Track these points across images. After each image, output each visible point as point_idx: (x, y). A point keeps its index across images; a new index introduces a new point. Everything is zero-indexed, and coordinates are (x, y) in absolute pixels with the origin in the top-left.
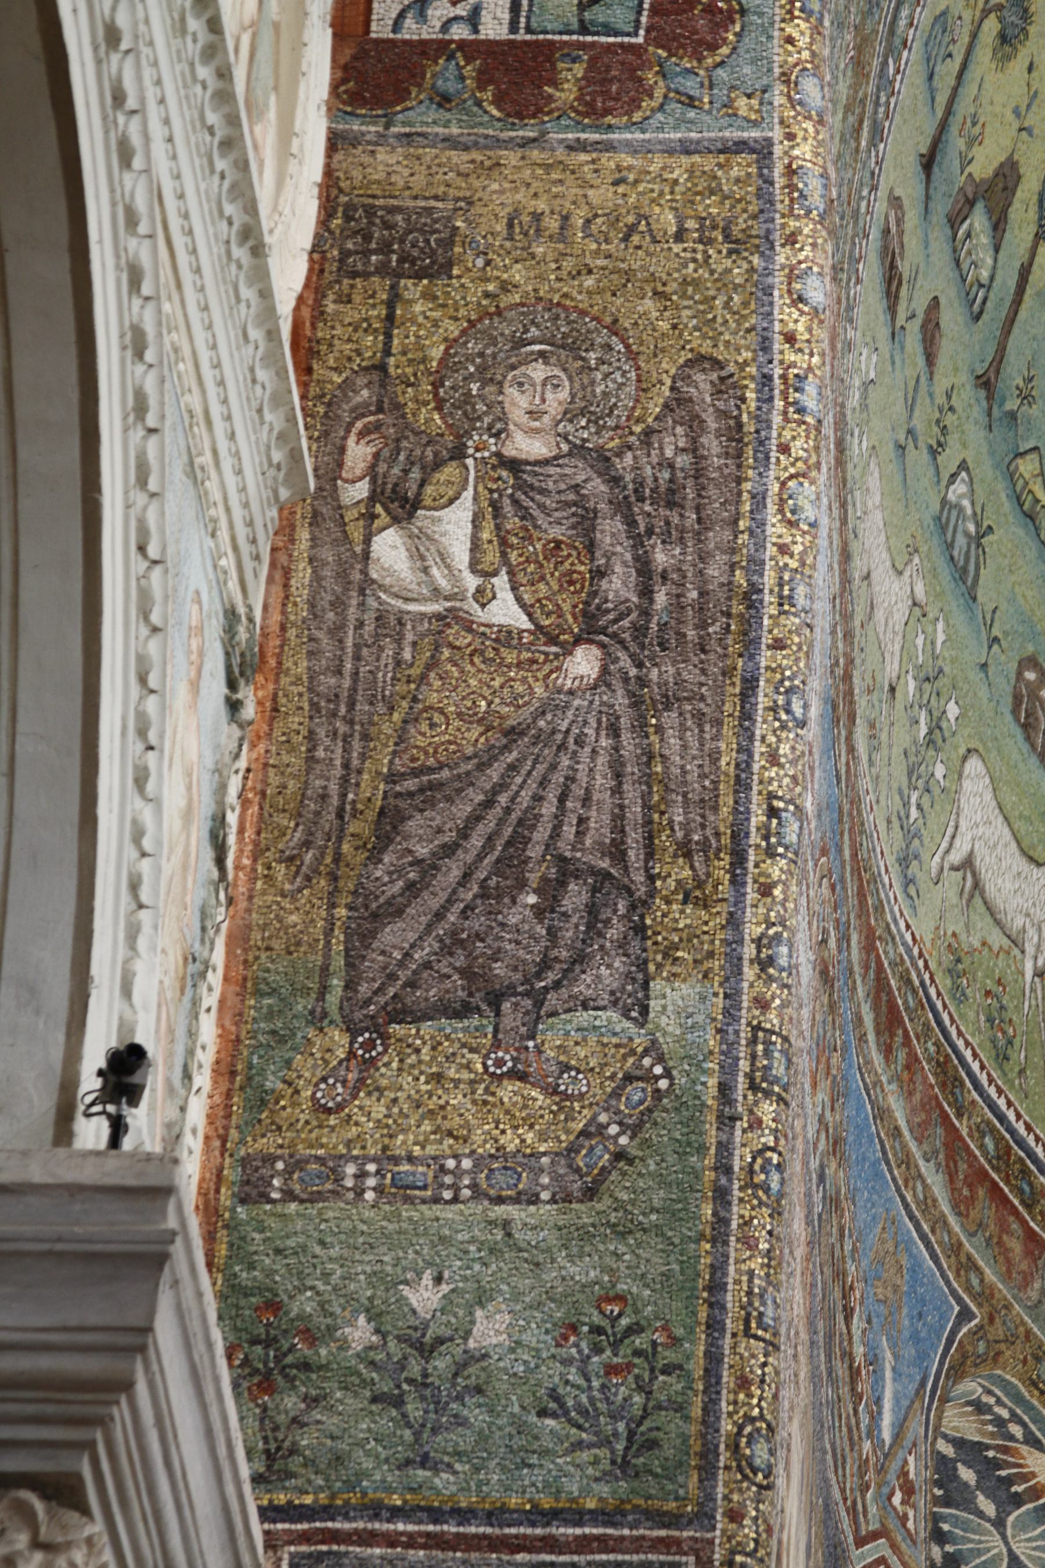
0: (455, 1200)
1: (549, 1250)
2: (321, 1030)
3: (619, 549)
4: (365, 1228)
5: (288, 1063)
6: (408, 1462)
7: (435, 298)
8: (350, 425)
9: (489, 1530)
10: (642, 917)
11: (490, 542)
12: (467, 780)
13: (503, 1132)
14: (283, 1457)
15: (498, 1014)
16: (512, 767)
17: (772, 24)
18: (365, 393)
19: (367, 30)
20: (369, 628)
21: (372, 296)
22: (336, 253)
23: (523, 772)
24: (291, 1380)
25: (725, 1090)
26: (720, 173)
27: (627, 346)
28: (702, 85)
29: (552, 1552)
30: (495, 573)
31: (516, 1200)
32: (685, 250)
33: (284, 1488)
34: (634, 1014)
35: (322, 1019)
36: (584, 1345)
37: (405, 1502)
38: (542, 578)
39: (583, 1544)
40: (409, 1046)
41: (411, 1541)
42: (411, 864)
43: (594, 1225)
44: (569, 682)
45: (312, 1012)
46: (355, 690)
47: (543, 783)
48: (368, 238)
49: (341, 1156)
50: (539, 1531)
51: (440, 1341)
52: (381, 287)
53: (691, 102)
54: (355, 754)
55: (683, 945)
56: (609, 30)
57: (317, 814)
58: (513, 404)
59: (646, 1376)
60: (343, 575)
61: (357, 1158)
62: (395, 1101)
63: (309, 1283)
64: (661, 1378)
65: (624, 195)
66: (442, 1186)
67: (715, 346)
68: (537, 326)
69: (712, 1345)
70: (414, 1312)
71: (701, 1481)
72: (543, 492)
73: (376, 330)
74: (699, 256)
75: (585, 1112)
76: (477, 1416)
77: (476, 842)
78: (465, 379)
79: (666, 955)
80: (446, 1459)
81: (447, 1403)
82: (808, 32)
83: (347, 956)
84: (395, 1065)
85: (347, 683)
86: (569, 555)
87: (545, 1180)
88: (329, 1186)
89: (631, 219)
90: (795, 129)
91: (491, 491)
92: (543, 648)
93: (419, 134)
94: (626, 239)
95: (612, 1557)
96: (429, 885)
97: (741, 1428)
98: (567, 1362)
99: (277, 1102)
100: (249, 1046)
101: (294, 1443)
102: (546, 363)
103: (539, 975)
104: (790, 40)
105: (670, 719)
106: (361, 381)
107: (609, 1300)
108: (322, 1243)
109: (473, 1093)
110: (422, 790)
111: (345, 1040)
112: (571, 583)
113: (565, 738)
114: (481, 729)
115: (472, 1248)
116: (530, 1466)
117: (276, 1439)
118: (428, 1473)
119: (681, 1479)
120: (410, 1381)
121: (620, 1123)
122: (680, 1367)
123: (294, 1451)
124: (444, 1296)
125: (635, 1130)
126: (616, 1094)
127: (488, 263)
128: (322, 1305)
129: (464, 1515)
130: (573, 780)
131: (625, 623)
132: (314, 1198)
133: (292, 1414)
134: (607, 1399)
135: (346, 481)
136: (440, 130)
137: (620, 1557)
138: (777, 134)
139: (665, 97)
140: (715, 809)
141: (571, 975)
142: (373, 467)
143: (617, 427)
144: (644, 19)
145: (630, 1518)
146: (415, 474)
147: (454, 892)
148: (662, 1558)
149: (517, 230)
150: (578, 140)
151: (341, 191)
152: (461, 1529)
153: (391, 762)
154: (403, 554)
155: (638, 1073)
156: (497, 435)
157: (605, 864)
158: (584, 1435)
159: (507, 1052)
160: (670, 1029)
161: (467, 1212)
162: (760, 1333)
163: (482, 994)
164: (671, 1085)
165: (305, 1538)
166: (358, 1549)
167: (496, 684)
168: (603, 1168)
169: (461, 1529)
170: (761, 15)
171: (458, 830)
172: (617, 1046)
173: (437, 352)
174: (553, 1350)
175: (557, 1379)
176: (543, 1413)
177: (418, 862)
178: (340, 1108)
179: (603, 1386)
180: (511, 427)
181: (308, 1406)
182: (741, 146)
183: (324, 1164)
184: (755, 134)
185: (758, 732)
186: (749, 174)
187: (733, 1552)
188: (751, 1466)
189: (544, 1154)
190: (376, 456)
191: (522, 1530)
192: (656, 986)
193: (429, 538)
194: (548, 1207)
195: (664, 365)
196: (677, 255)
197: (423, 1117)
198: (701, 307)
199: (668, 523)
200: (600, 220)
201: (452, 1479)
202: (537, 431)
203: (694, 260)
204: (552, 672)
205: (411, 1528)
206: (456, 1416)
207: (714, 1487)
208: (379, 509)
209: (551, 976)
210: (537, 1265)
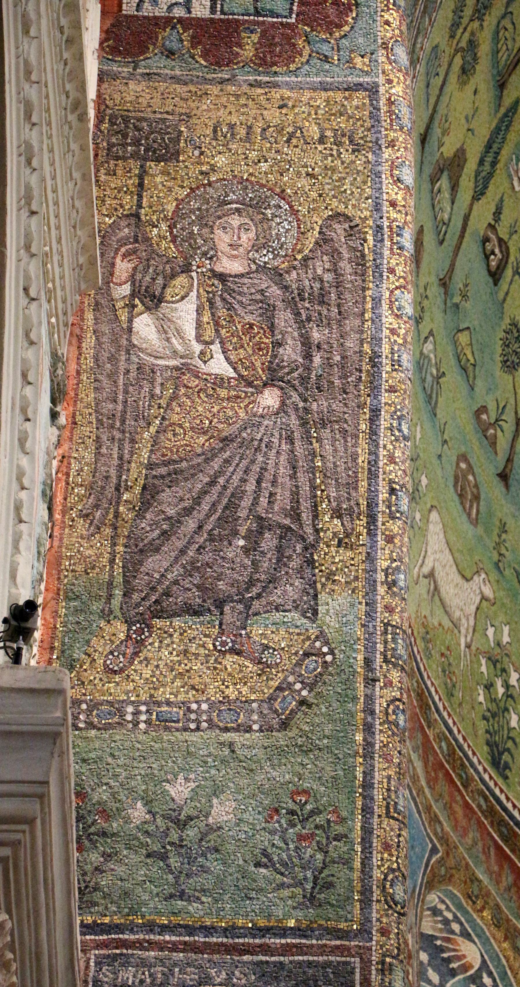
0: (198, 729)
1: (259, 761)
2: (109, 622)
3: (289, 329)
4: (140, 746)
5: (88, 642)
6: (171, 896)
7: (169, 174)
8: (118, 250)
9: (225, 940)
10: (312, 554)
11: (208, 323)
12: (198, 469)
13: (227, 687)
14: (90, 892)
15: (222, 613)
16: (227, 461)
17: (376, 12)
18: (126, 230)
19: (120, 10)
20: (133, 374)
21: (129, 172)
22: (105, 144)
23: (234, 464)
24: (94, 843)
25: (368, 662)
26: (346, 103)
27: (291, 207)
28: (333, 49)
29: (266, 955)
30: (212, 343)
31: (237, 730)
32: (325, 149)
33: (91, 912)
34: (309, 615)
35: (109, 615)
36: (283, 821)
37: (170, 921)
38: (242, 347)
39: (287, 950)
40: (165, 632)
41: (174, 948)
42: (164, 520)
43: (287, 746)
44: (261, 410)
45: (103, 611)
46: (125, 412)
47: (247, 471)
48: (125, 136)
49: (123, 701)
50: (257, 941)
51: (190, 818)
52: (134, 166)
53: (326, 59)
54: (126, 451)
55: (339, 571)
56: (273, 14)
57: (103, 488)
58: (220, 239)
59: (324, 841)
60: (115, 341)
61: (133, 702)
62: (157, 666)
63: (105, 781)
64: (334, 843)
65: (286, 115)
66: (189, 720)
67: (346, 207)
68: (234, 193)
69: (365, 823)
70: (173, 800)
71: (361, 909)
72: (240, 293)
73: (132, 192)
74: (335, 153)
75: (280, 675)
76: (216, 867)
77: (205, 507)
78: (189, 224)
79: (328, 579)
80: (197, 894)
81: (196, 858)
82: (398, 18)
83: (124, 575)
84: (156, 645)
85: (120, 407)
86: (259, 333)
87: (255, 717)
88: (116, 719)
89: (290, 129)
90: (391, 77)
91: (208, 292)
92: (243, 389)
93: (155, 74)
94: (288, 141)
95: (305, 958)
96: (176, 533)
97: (386, 876)
98: (272, 832)
99: (81, 667)
100: (62, 631)
101: (97, 884)
102: (239, 215)
103: (247, 590)
104: (387, 23)
105: (326, 433)
106: (123, 223)
107: (299, 793)
108: (112, 755)
109: (207, 662)
110: (169, 474)
111: (124, 628)
112: (260, 349)
113: (260, 444)
114: (206, 437)
115: (210, 760)
116: (250, 899)
117: (85, 882)
118: (185, 903)
119: (349, 908)
120: (172, 844)
121: (302, 682)
122: (346, 836)
123: (96, 889)
124: (192, 790)
125: (311, 687)
126: (299, 664)
127: (202, 153)
128: (113, 795)
129: (209, 930)
130: (266, 470)
131: (295, 375)
132: (107, 727)
133: (95, 864)
134: (299, 856)
135: (116, 284)
136: (169, 72)
137: (311, 958)
138: (381, 80)
139: (310, 56)
140: (356, 489)
141: (268, 590)
142: (133, 276)
143: (286, 255)
144: (295, 8)
145: (317, 933)
146: (160, 281)
147: (192, 537)
148: (338, 959)
149: (220, 134)
150: (256, 80)
151: (107, 106)
152: (207, 939)
153: (149, 457)
154: (154, 329)
155: (313, 651)
156: (211, 258)
157: (287, 522)
158: (285, 879)
159: (228, 637)
160: (332, 624)
161: (205, 737)
162: (396, 815)
163: (212, 601)
164: (334, 658)
165: (104, 945)
166: (140, 953)
167: (215, 410)
168: (292, 710)
169: (207, 939)
170: (369, 7)
171: (194, 500)
172: (298, 634)
173: (171, 207)
174: (263, 825)
175: (266, 843)
176: (258, 865)
177: (169, 518)
178: (122, 671)
179: (297, 848)
180: (220, 254)
181: (105, 860)
182: (359, 87)
183: (112, 706)
184: (367, 79)
185: (381, 442)
186: (364, 104)
187: (384, 956)
188: (393, 899)
189: (254, 701)
190: (135, 269)
191: (247, 940)
192: (323, 597)
193: (169, 320)
194: (258, 734)
195: (314, 218)
196: (321, 152)
197: (175, 677)
198: (337, 184)
199: (320, 314)
200: (271, 130)
201: (200, 907)
202: (235, 257)
203: (332, 155)
204: (250, 403)
205: (174, 938)
206: (201, 866)
207: (370, 913)
208: (137, 301)
209: (255, 591)
210: (252, 770)
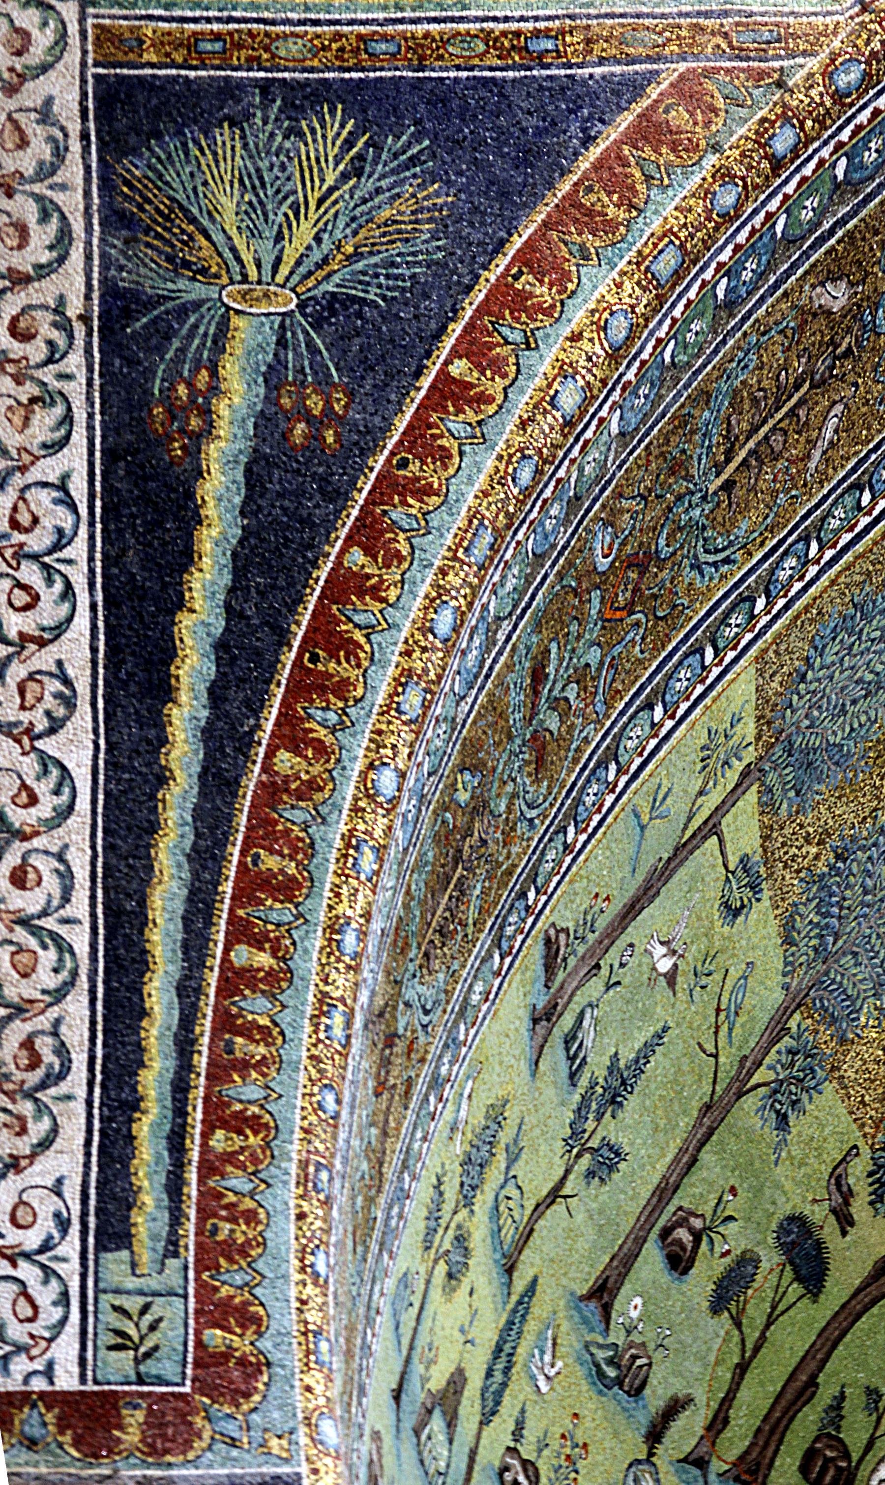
17: (293, 1374)
28: (241, 1428)
53: (233, 1443)
56: (161, 1381)
82: (322, 1381)
90: (319, 1465)
104: (308, 1389)
136: (31, 1470)
139: (212, 1438)
144: (189, 1371)
170: (283, 1367)
